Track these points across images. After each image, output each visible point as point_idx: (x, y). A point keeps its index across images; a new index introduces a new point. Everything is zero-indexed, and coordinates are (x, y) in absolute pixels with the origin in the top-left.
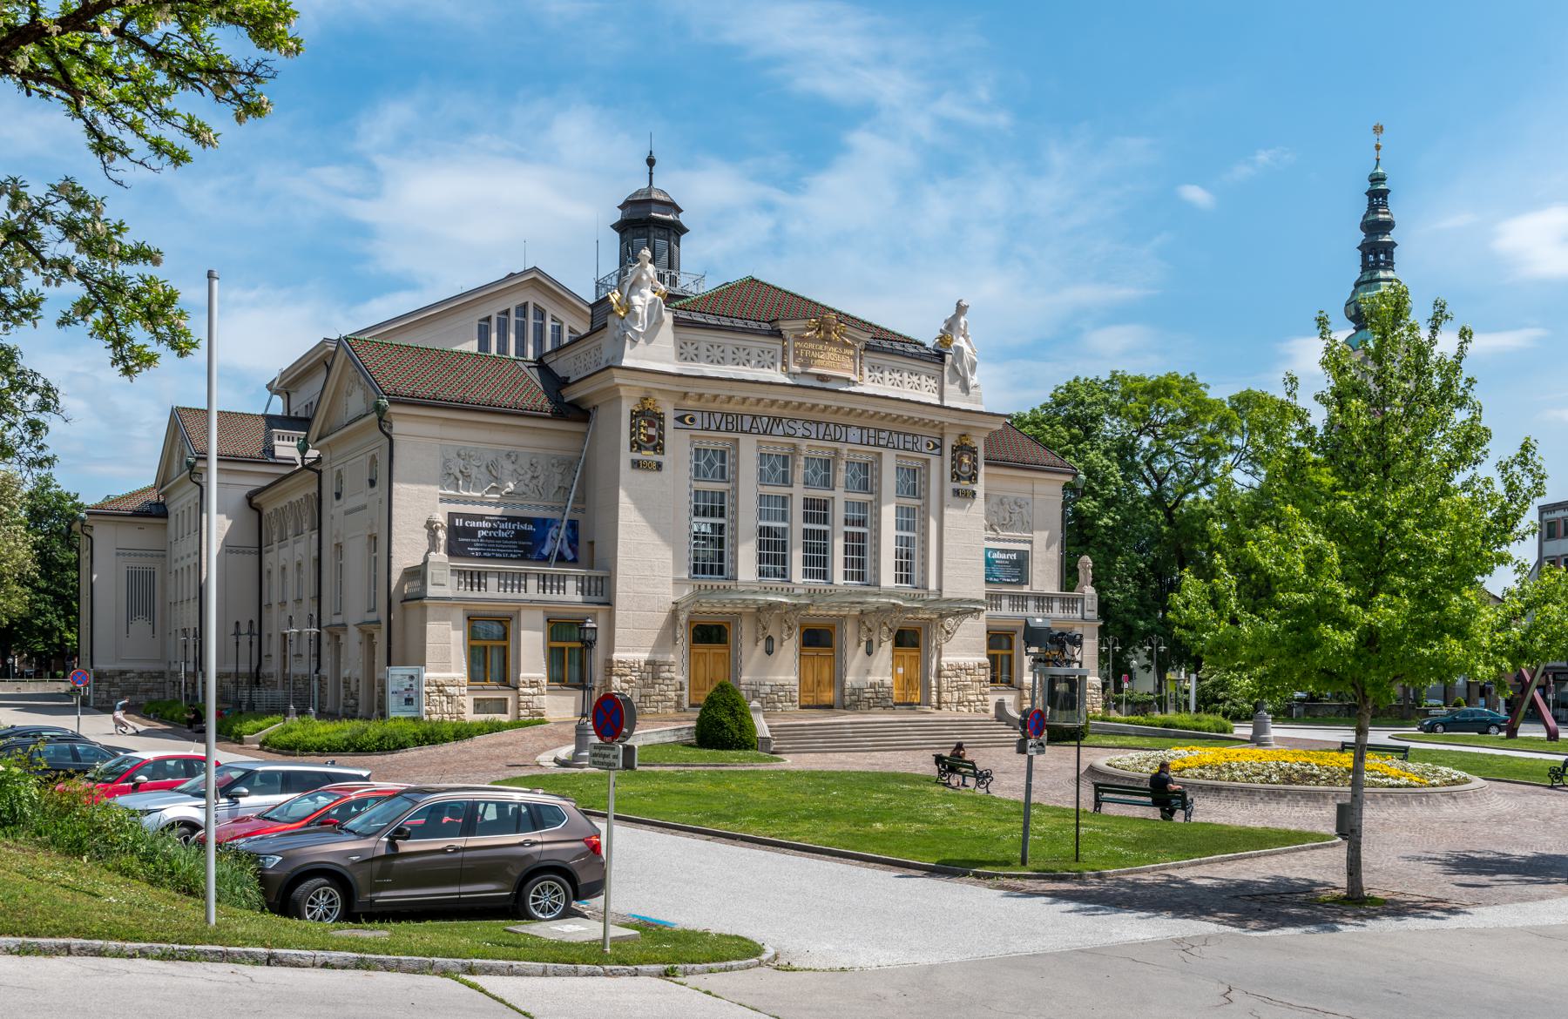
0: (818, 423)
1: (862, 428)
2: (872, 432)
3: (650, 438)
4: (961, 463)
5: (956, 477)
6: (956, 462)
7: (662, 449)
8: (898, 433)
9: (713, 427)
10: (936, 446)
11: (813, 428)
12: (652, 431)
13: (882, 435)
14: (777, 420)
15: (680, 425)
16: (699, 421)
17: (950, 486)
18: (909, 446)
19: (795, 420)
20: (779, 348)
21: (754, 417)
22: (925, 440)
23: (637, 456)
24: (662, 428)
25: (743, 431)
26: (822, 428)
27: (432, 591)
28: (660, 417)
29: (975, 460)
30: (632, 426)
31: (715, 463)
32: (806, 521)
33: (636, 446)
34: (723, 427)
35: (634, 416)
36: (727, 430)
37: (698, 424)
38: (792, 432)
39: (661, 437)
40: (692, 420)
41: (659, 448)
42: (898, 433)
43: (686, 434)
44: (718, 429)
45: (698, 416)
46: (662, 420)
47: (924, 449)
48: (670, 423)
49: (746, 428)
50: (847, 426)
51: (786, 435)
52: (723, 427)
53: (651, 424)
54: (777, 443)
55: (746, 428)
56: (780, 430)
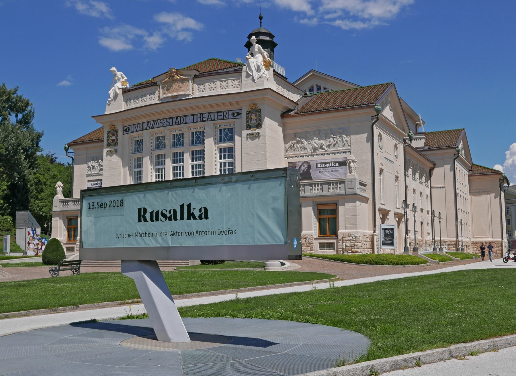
0: (172, 118)
1: (193, 115)
3: (113, 141)
4: (251, 119)
6: (249, 119)
8: (214, 113)
10: (239, 114)
11: (170, 121)
12: (114, 138)
13: (204, 116)
14: (156, 121)
15: (125, 132)
18: (219, 117)
21: (148, 122)
22: (231, 113)
24: (117, 136)
25: (144, 130)
26: (174, 120)
27: (54, 209)
31: (139, 145)
32: (193, 161)
34: (138, 130)
35: (109, 133)
37: (130, 131)
38: (162, 125)
39: (117, 139)
41: (116, 144)
45: (130, 127)
46: (117, 132)
47: (231, 116)
48: (120, 133)
50: (186, 116)
51: (160, 127)
52: (138, 130)
53: (113, 135)
54: (158, 131)
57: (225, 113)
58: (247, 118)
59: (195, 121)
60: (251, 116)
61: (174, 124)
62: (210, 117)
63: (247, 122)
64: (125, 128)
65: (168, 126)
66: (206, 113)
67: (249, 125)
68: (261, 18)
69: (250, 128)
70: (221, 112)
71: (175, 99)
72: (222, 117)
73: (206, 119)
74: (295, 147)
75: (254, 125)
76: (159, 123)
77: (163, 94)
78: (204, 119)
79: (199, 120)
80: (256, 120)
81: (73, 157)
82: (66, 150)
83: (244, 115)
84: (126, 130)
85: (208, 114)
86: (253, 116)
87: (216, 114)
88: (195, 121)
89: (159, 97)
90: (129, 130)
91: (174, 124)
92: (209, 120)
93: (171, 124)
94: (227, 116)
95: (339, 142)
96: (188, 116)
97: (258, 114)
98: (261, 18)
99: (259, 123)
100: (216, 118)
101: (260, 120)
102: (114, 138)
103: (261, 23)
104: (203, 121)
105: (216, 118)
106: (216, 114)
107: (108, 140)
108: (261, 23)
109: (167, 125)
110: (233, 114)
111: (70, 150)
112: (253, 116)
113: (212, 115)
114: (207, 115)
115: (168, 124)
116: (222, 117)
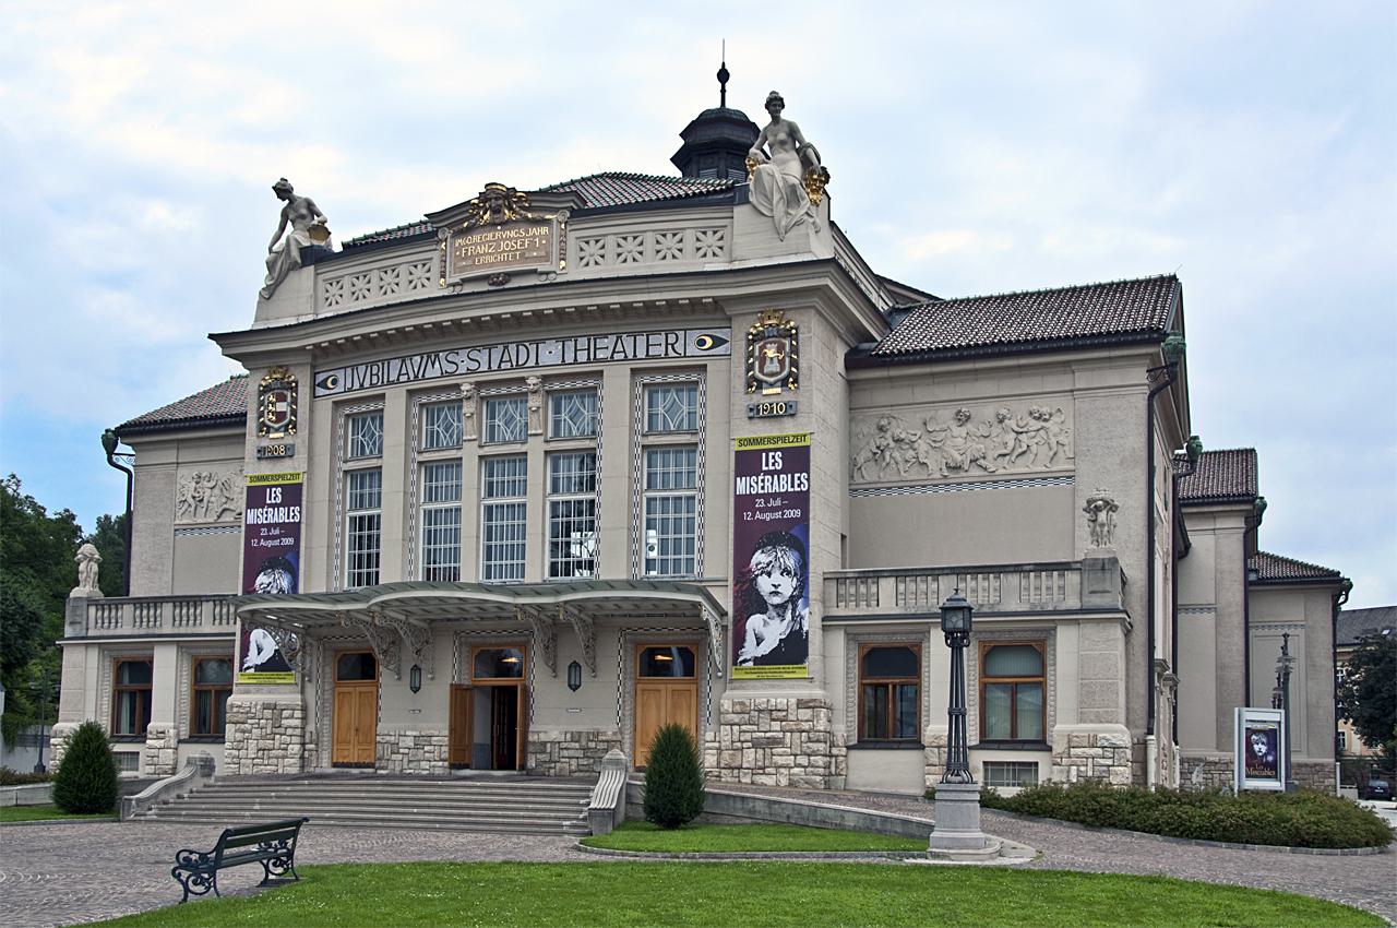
2: (583, 343)
3: (280, 416)
4: (763, 359)
5: (755, 384)
6: (754, 360)
7: (295, 427)
9: (357, 386)
10: (718, 342)
11: (483, 357)
12: (282, 407)
15: (320, 391)
16: (341, 382)
17: (742, 401)
19: (454, 351)
20: (436, 255)
23: (265, 443)
24: (295, 401)
25: (389, 383)
26: (496, 354)
29: (795, 350)
33: (264, 428)
34: (367, 384)
39: (294, 413)
40: (334, 382)
42: (629, 334)
46: (295, 390)
47: (692, 350)
52: (367, 384)
53: (281, 398)
57: (672, 339)
58: (750, 355)
59: (569, 358)
60: (764, 347)
61: (494, 367)
62: (619, 348)
63: (750, 368)
64: (320, 378)
65: (474, 372)
66: (606, 336)
67: (754, 378)
69: (760, 387)
70: (658, 332)
71: (499, 283)
72: (661, 351)
73: (608, 354)
74: (888, 458)
75: (772, 380)
76: (444, 362)
78: (600, 355)
79: (582, 356)
80: (782, 362)
81: (132, 469)
82: (110, 442)
83: (738, 347)
84: (323, 385)
85: (614, 337)
86: (771, 352)
87: (641, 340)
88: (569, 358)
90: (334, 382)
91: (494, 367)
92: (616, 356)
93: (484, 367)
94: (679, 348)
95: (1034, 448)
96: (543, 341)
97: (787, 342)
99: (790, 374)
100: (641, 353)
101: (794, 363)
102: (282, 407)
104: (597, 360)
105: (641, 353)
106: (641, 340)
107: (261, 415)
110: (702, 343)
111: (121, 448)
112: (771, 352)
113: (628, 342)
114: (609, 342)
115: (474, 366)
116: (661, 351)
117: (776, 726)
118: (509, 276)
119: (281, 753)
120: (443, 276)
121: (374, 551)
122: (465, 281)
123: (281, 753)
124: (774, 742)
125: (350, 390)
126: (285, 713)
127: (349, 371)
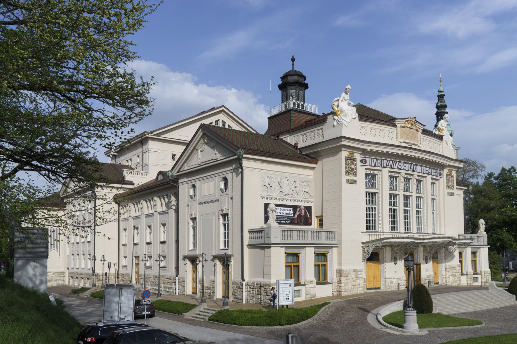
3: (352, 169)
9: (373, 165)
11: (407, 165)
16: (368, 162)
24: (356, 165)
25: (384, 167)
28: (355, 160)
30: (346, 164)
36: (378, 166)
37: (367, 164)
38: (400, 167)
39: (356, 169)
43: (364, 167)
44: (375, 166)
48: (358, 163)
49: (385, 165)
52: (377, 165)
55: (385, 165)
56: (395, 167)
68: (293, 60)
77: (401, 138)
78: (427, 172)
89: (397, 138)
98: (293, 60)
103: (293, 64)
108: (293, 64)
109: (404, 170)
115: (405, 168)
117: (455, 271)
118: (414, 144)
119: (358, 286)
120: (397, 138)
121: (368, 219)
122: (404, 142)
123: (358, 286)
124: (455, 275)
125: (371, 166)
126: (359, 273)
127: (370, 159)
